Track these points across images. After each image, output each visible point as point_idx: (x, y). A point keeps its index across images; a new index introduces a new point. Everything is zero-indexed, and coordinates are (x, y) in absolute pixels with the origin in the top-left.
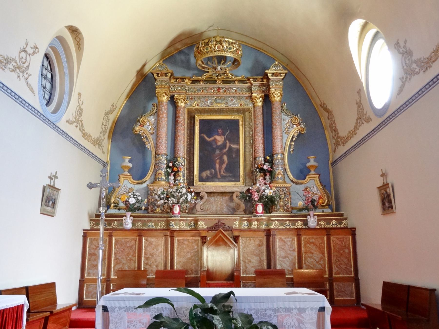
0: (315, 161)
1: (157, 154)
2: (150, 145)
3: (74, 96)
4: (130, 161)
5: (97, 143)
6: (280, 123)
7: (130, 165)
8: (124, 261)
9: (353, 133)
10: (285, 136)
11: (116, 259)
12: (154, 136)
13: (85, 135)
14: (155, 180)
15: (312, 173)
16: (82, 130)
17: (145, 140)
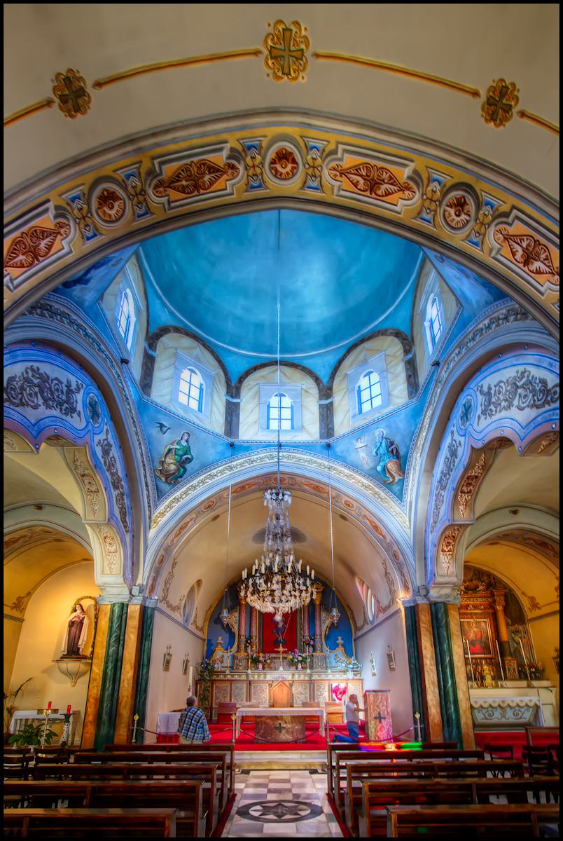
0: (342, 639)
1: (239, 635)
2: (235, 629)
3: (194, 610)
4: (222, 639)
5: (201, 630)
6: (320, 617)
7: (222, 642)
8: (221, 698)
9: (362, 627)
10: (323, 625)
11: (216, 696)
12: (237, 625)
13: (197, 628)
14: (238, 651)
15: (340, 646)
16: (196, 626)
17: (231, 627)
